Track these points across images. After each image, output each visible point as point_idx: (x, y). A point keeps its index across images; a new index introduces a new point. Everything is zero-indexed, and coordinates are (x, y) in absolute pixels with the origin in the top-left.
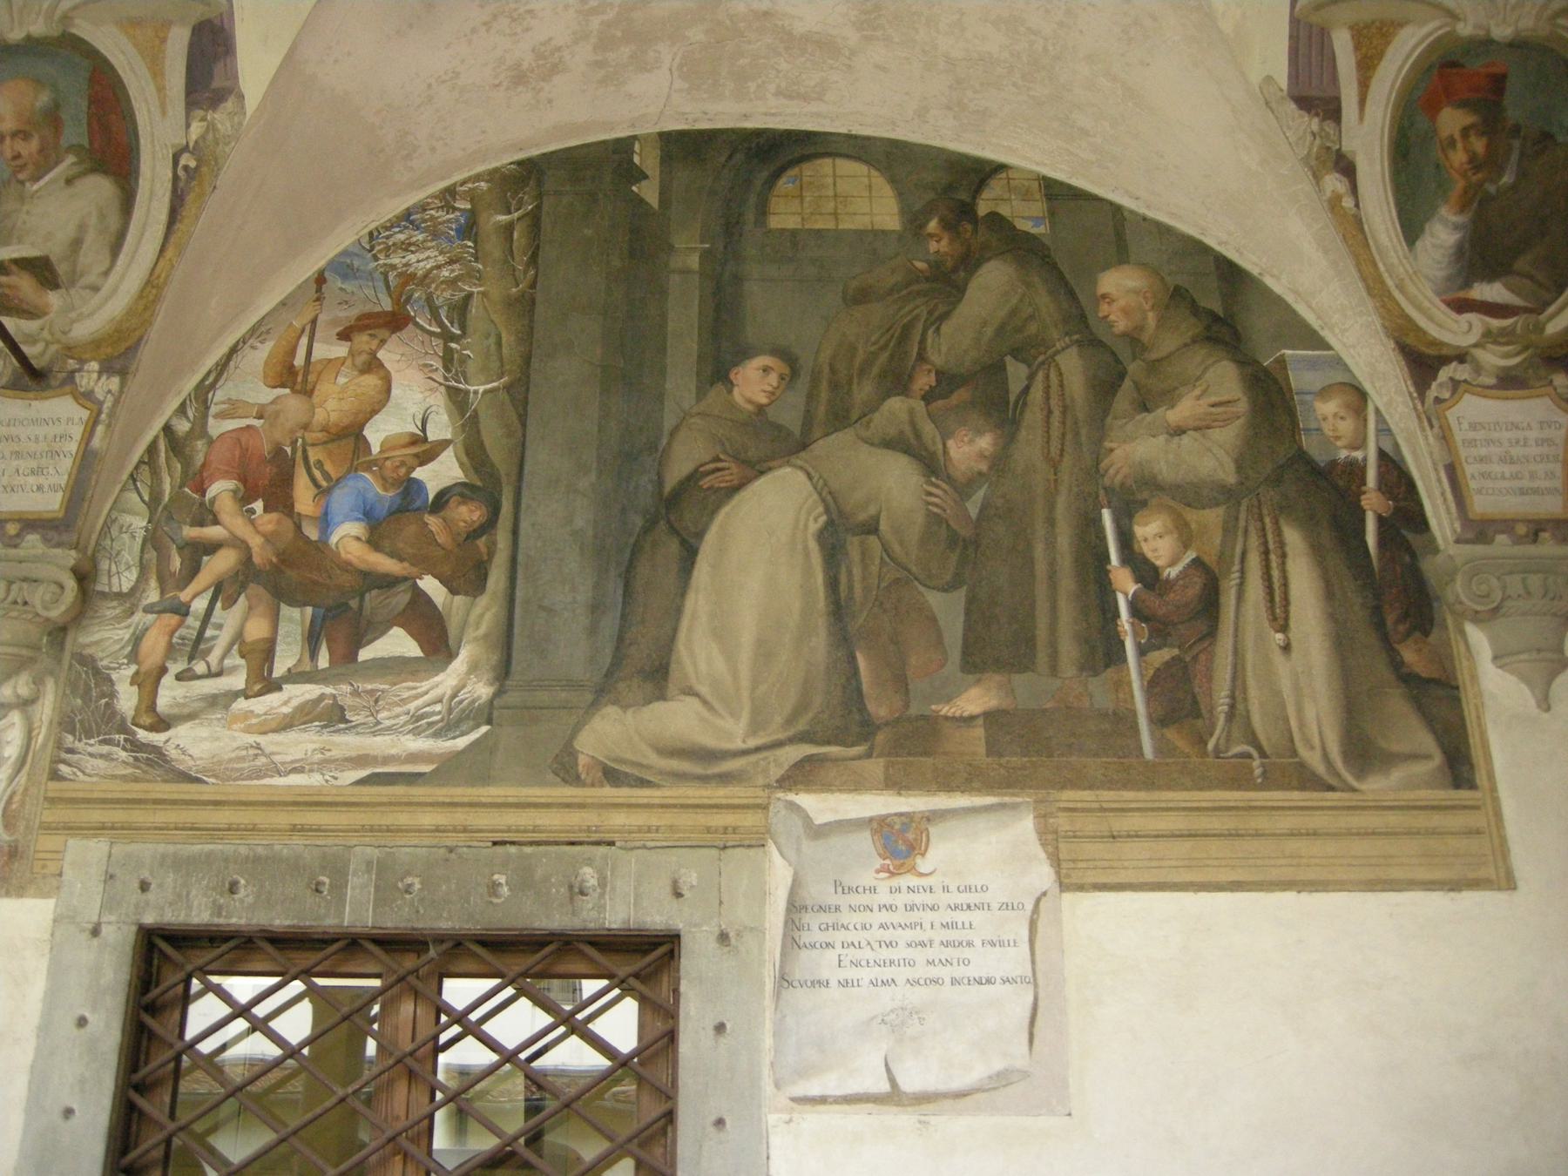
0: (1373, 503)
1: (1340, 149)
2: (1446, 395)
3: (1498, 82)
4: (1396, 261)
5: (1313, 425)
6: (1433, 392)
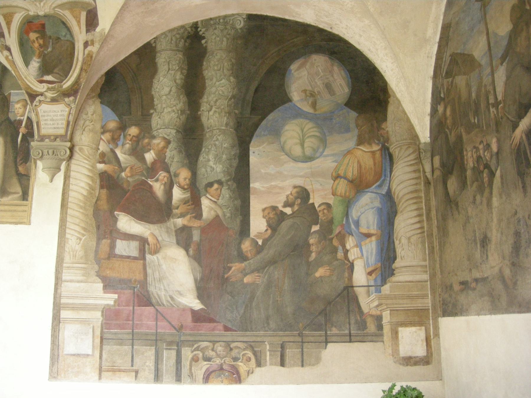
0: (22, 130)
1: (6, 45)
2: (38, 104)
3: (43, 26)
4: (24, 71)
5: (13, 110)
6: (35, 103)
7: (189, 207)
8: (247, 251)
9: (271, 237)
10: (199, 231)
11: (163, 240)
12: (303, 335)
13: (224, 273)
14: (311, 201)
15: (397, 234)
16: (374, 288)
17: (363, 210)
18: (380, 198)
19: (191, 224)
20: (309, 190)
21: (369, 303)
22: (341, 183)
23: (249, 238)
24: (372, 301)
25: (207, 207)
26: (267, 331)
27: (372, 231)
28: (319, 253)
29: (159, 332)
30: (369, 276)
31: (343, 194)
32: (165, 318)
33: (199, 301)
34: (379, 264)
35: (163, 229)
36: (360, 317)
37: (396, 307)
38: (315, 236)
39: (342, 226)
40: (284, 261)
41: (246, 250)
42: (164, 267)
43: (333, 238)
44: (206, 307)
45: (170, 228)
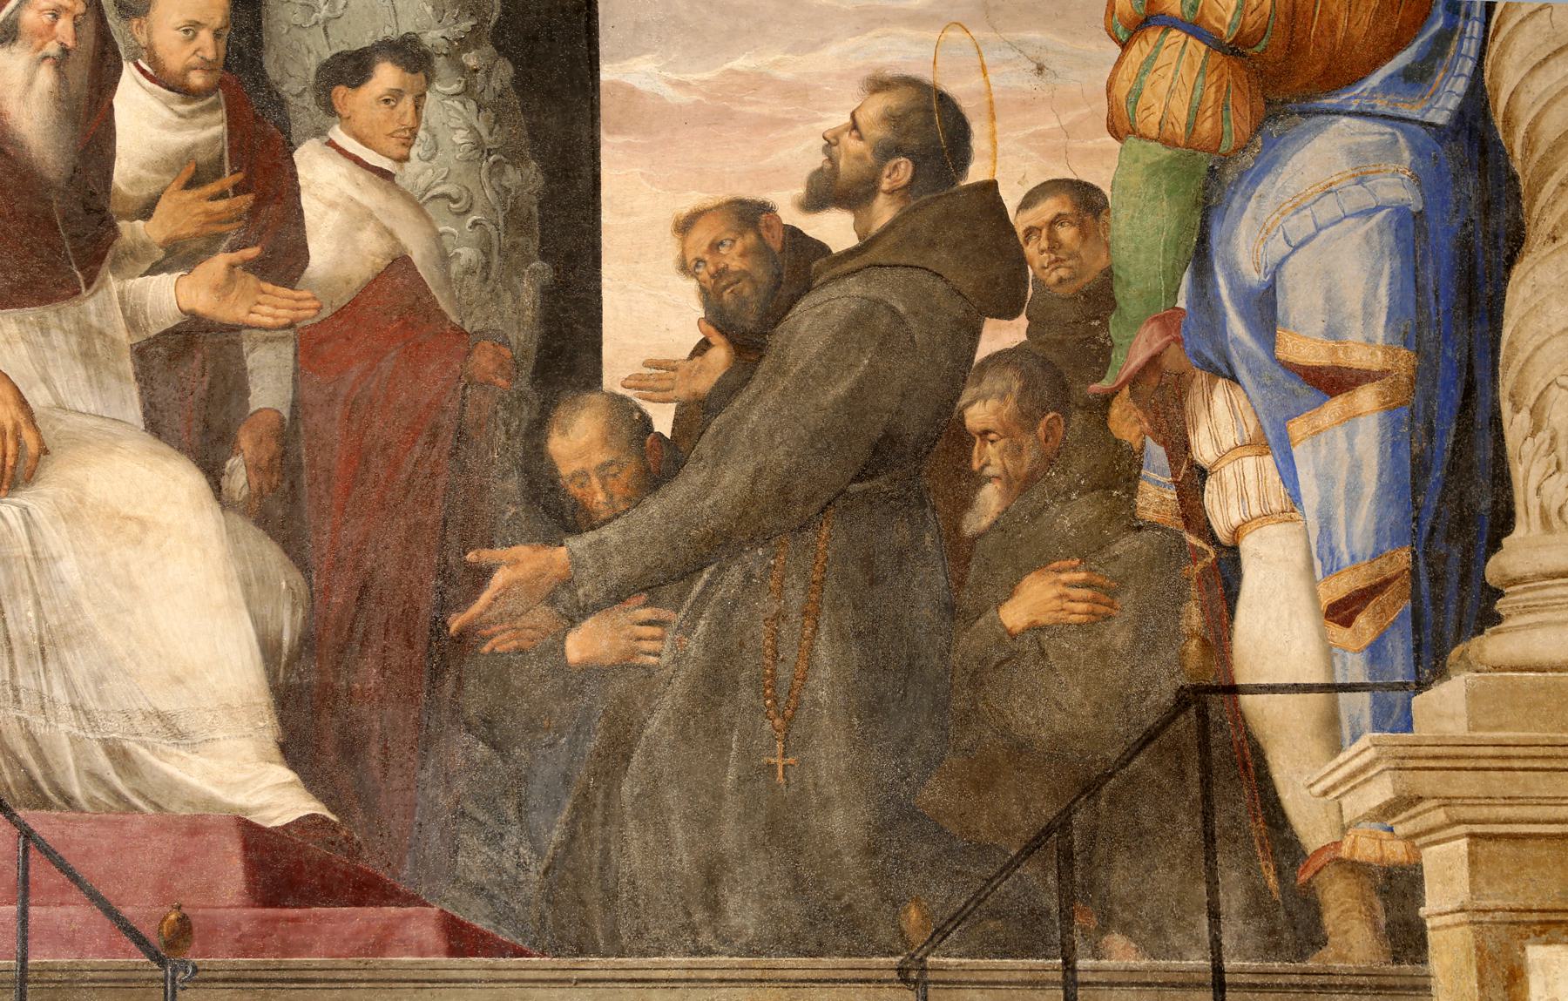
7: (221, 205)
8: (584, 473)
9: (726, 391)
10: (288, 351)
11: (61, 407)
12: (930, 976)
13: (445, 607)
14: (976, 173)
15: (1521, 371)
16: (1365, 698)
17: (1301, 225)
18: (1418, 151)
19: (233, 310)
20: (967, 106)
21: (1334, 787)
22: (1165, 56)
23: (594, 397)
24: (1353, 775)
25: (332, 205)
26: (710, 952)
27: (1360, 357)
28: (1021, 486)
29: (43, 969)
30: (1335, 630)
31: (1180, 130)
32: (75, 879)
33: (289, 775)
34: (1403, 558)
35: (57, 337)
36: (1279, 873)
37: (1508, 821)
38: (999, 386)
39: (1169, 320)
40: (809, 534)
41: (577, 466)
42: (69, 569)
43: (1115, 393)
44: (333, 811)
45: (101, 333)
